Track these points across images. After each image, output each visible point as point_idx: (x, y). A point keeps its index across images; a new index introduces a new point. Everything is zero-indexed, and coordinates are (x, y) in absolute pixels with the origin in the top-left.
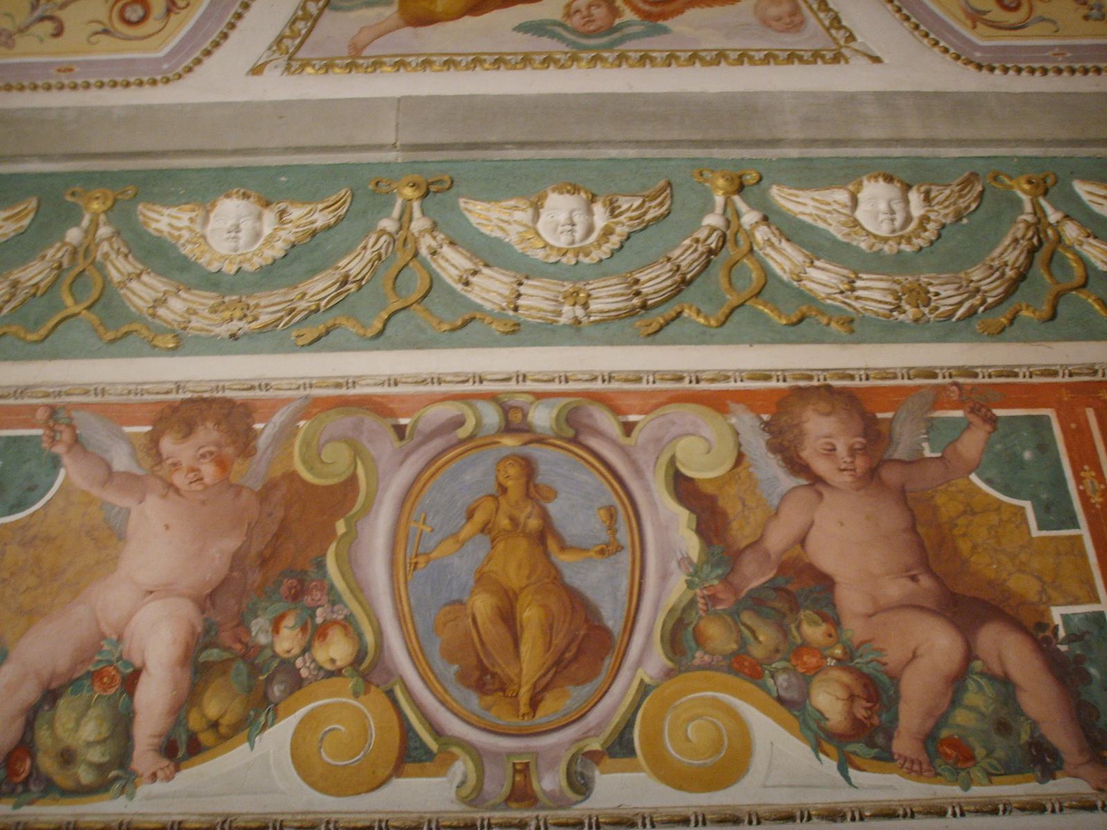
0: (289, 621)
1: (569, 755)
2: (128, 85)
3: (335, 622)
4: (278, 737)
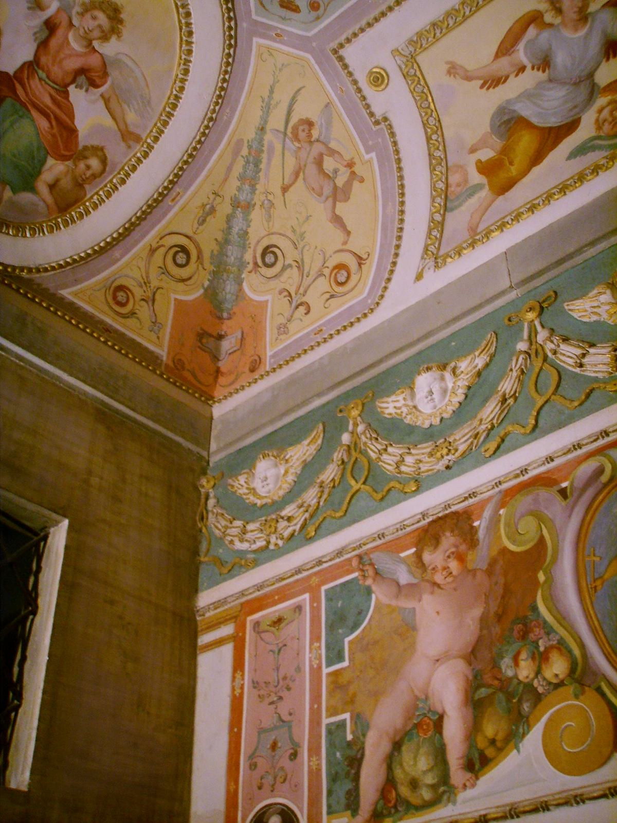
0: (523, 655)
2: (352, 324)
3: (552, 647)
4: (533, 739)
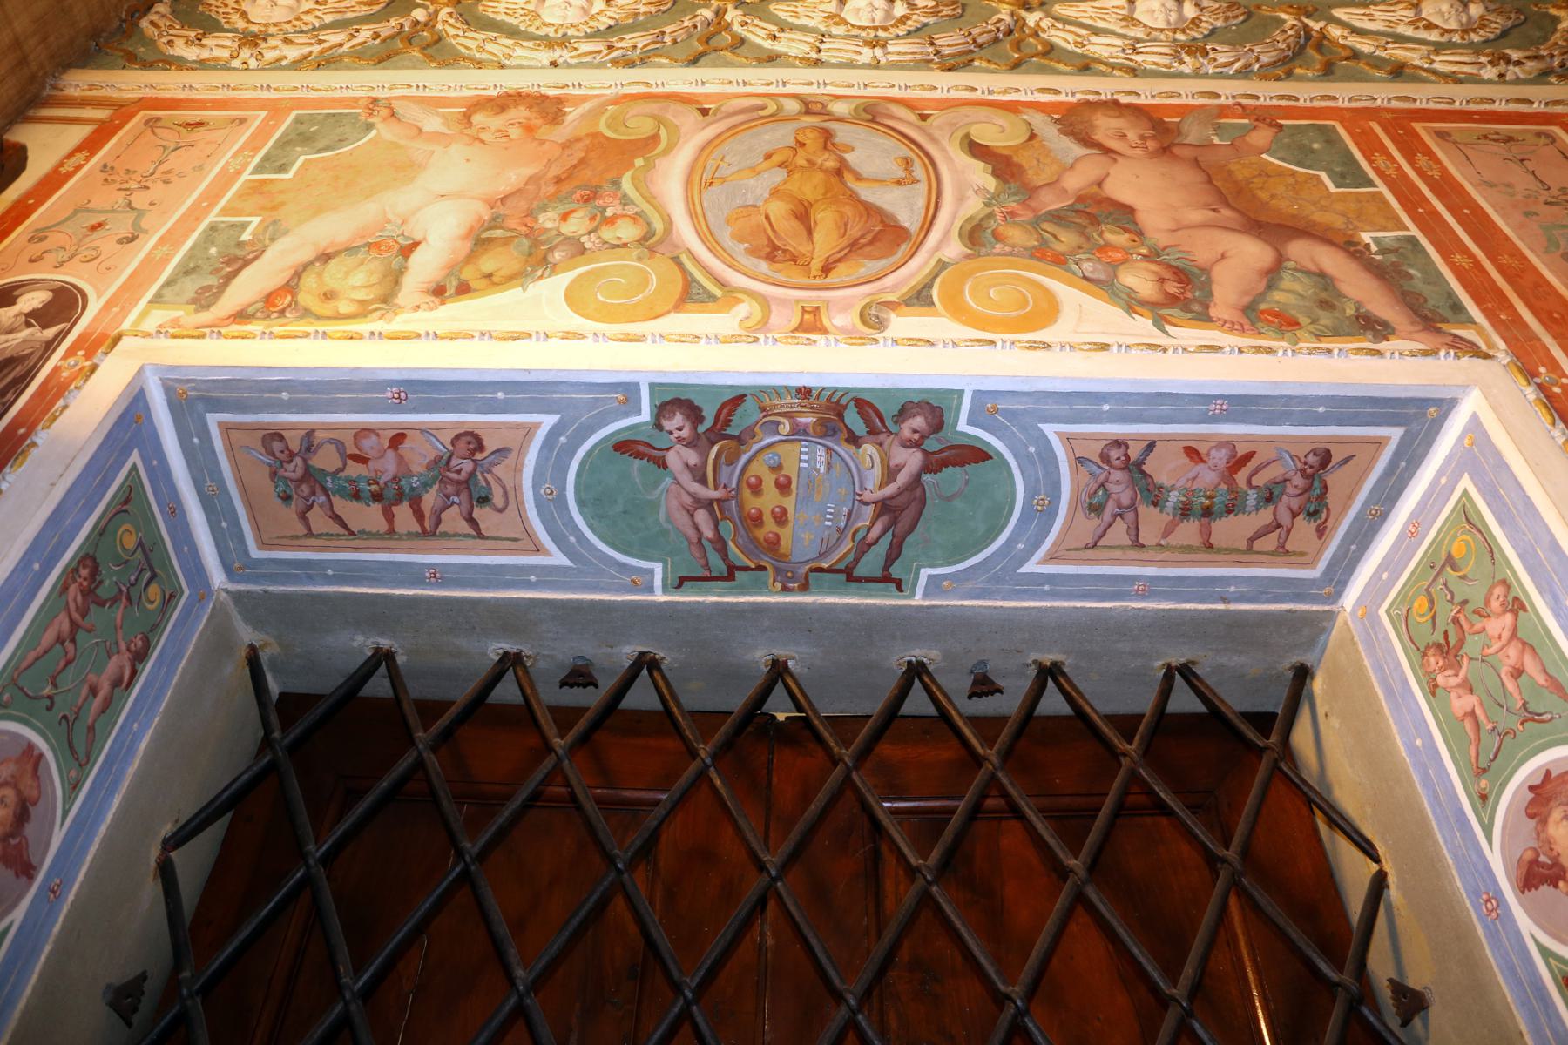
1: (863, 303)
